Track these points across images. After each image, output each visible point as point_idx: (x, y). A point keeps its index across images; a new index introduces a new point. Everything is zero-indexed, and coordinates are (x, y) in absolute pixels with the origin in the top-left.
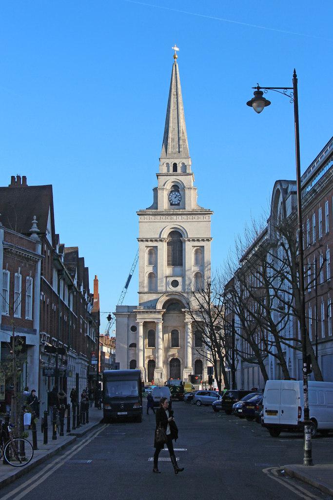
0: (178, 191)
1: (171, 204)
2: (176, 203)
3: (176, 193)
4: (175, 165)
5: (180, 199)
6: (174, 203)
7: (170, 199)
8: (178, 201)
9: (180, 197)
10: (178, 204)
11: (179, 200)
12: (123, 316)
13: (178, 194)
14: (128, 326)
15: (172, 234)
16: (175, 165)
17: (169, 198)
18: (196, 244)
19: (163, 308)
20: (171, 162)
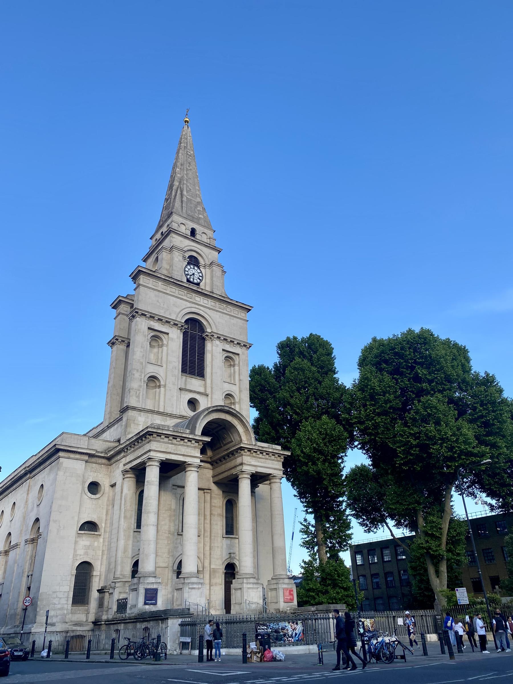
0: (199, 267)
1: (188, 280)
2: (195, 281)
3: (196, 268)
4: (193, 232)
5: (201, 278)
6: (192, 280)
7: (187, 273)
8: (199, 281)
9: (200, 274)
10: (198, 284)
11: (199, 279)
12: (78, 456)
13: (199, 272)
14: (84, 482)
15: (187, 321)
16: (193, 232)
17: (185, 271)
18: (228, 347)
19: (204, 433)
20: (191, 225)
